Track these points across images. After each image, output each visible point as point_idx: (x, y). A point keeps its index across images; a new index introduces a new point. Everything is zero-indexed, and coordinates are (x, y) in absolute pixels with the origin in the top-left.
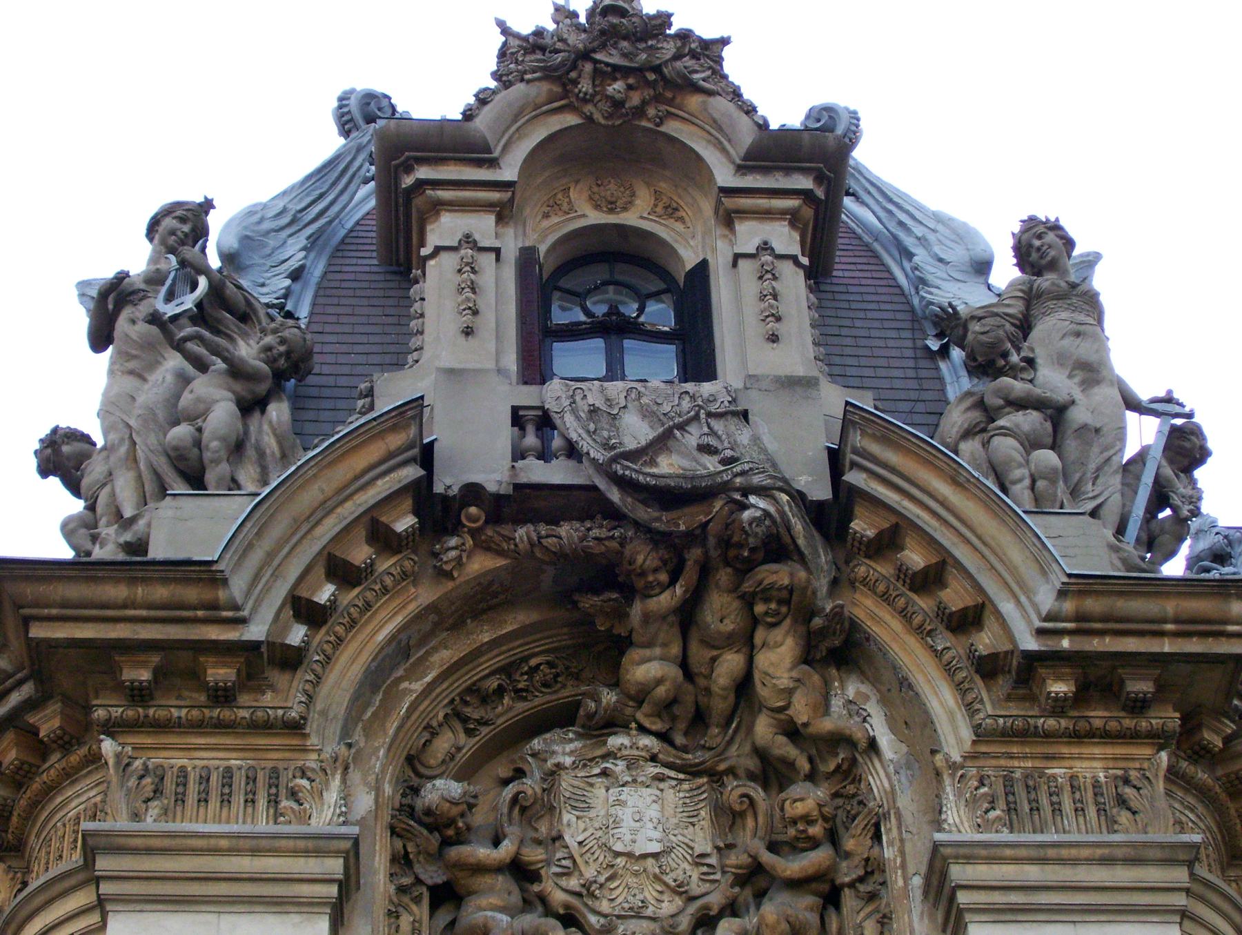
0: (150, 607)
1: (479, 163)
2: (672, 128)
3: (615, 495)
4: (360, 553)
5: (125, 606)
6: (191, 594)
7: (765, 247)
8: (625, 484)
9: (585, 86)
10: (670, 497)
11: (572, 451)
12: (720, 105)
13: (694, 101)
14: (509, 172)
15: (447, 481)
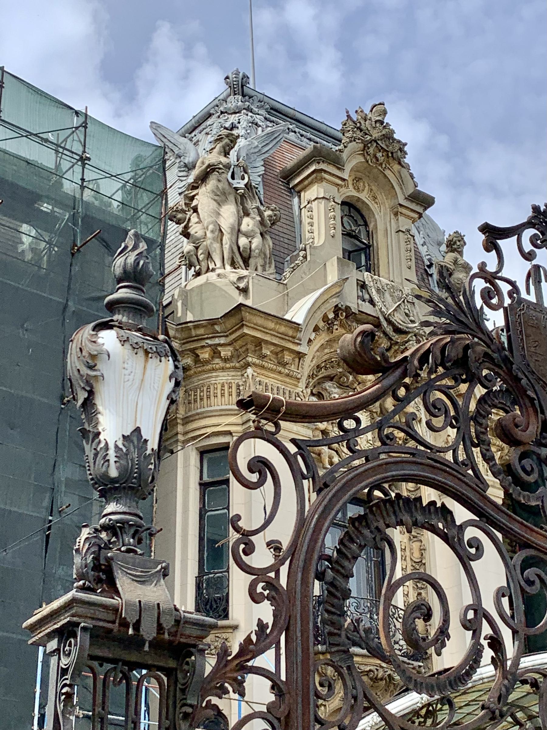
0: (278, 333)
1: (339, 169)
2: (387, 172)
3: (384, 324)
4: (321, 324)
5: (271, 330)
6: (290, 333)
7: (408, 231)
8: (389, 322)
9: (371, 151)
10: (398, 331)
11: (372, 302)
12: (404, 171)
13: (396, 167)
14: (346, 177)
15: (343, 304)
